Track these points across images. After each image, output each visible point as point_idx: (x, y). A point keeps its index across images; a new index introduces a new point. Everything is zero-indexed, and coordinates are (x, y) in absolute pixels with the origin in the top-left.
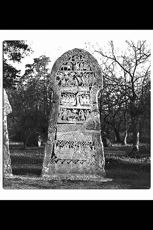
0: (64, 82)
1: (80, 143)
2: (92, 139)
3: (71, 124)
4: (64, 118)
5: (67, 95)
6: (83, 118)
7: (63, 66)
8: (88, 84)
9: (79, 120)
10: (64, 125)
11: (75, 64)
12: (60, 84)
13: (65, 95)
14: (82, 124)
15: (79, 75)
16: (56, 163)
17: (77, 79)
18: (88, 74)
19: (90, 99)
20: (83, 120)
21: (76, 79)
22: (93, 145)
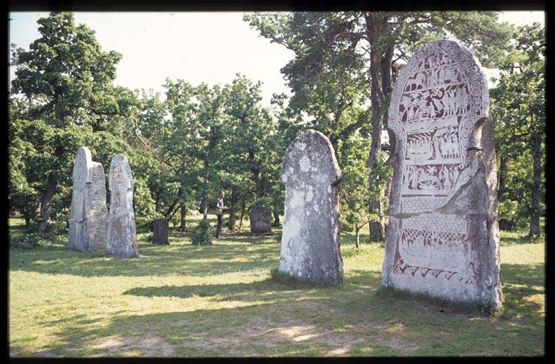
0: (410, 114)
4: (414, 185)
6: (447, 183)
7: (410, 83)
10: (412, 198)
12: (404, 118)
13: (414, 139)
17: (433, 104)
21: (431, 103)
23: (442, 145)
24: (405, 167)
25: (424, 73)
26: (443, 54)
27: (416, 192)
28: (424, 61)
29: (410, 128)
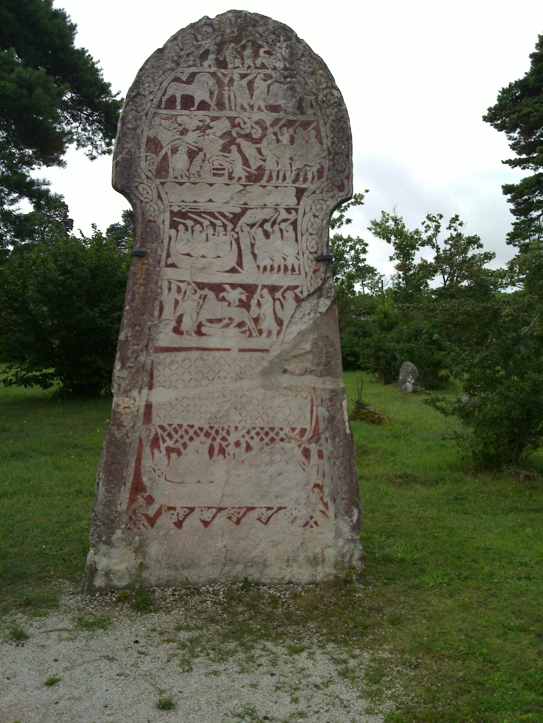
0: (179, 162)
1: (258, 434)
2: (308, 415)
3: (217, 354)
4: (187, 324)
5: (197, 222)
6: (269, 323)
7: (178, 91)
8: (288, 174)
9: (251, 335)
10: (183, 354)
11: (231, 80)
13: (190, 223)
14: (267, 351)
15: (250, 133)
16: (152, 526)
17: (240, 151)
18: (291, 131)
19: (297, 240)
20: (270, 333)
21: (234, 148)
22: (316, 437)
23: (258, 244)
24: (165, 285)
25: (213, 74)
26: (261, 47)
27: (192, 341)
28: (213, 48)
29: (177, 197)
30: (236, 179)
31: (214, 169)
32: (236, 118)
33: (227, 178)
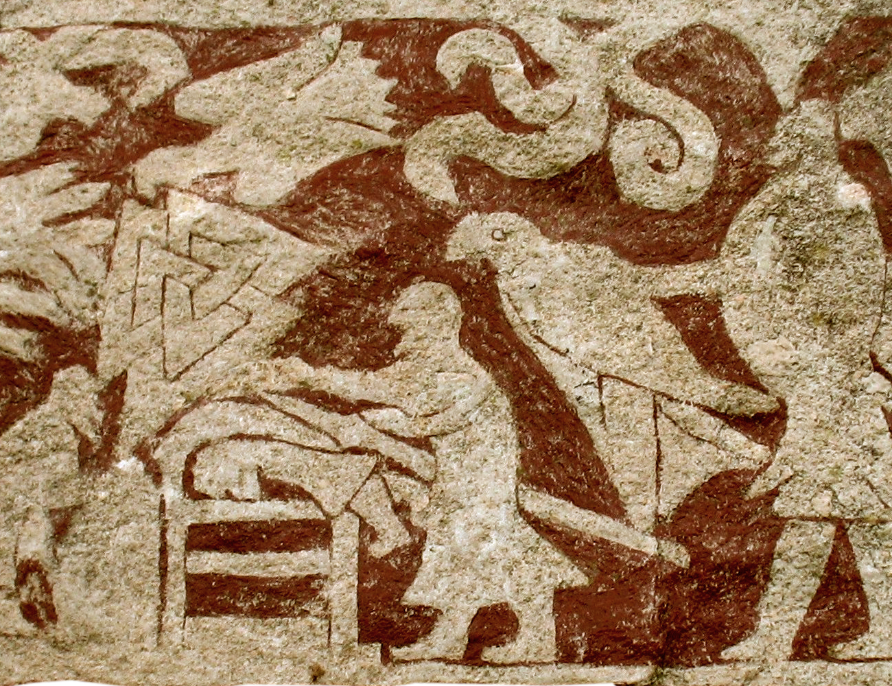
15: (598, 166)
17: (491, 335)
30: (450, 634)
31: (205, 537)
32: (449, 28)
33: (347, 625)
